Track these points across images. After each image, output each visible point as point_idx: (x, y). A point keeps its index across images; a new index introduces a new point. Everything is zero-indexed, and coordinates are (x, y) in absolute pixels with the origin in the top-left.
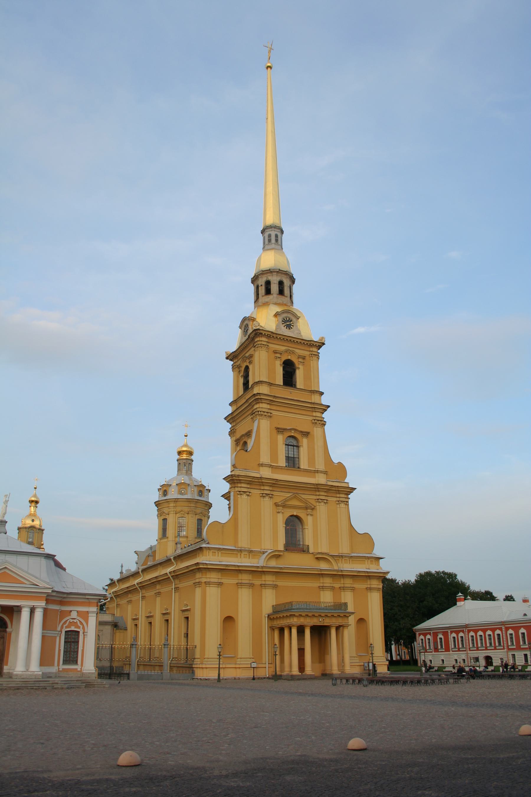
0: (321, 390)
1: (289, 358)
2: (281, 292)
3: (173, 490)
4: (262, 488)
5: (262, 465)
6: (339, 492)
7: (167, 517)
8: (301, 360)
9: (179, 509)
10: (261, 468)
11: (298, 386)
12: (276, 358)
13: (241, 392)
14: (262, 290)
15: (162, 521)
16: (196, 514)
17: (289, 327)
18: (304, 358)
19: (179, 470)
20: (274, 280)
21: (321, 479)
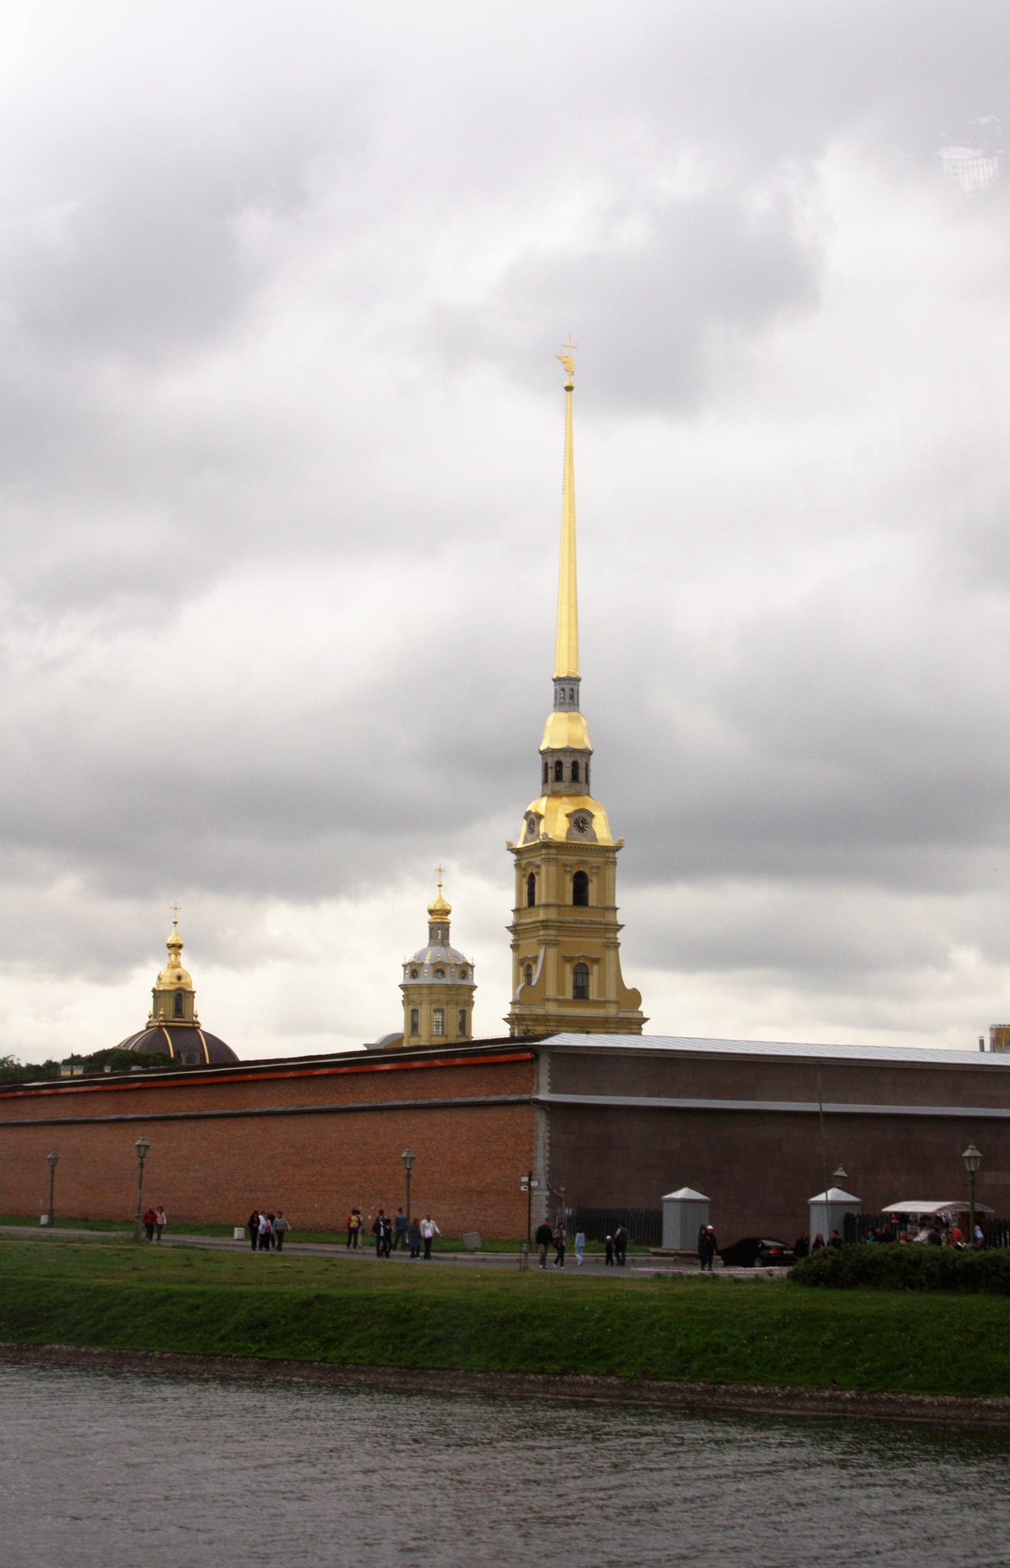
0: (617, 906)
1: (581, 869)
2: (575, 777)
3: (426, 971)
4: (547, 1024)
5: (548, 1000)
6: (631, 1023)
7: (418, 1007)
8: (594, 871)
9: (435, 997)
10: (547, 1003)
11: (590, 904)
12: (566, 872)
13: (525, 903)
14: (551, 774)
15: (410, 1012)
16: (457, 1005)
17: (582, 830)
18: (598, 868)
19: (431, 937)
20: (567, 762)
21: (612, 1011)
